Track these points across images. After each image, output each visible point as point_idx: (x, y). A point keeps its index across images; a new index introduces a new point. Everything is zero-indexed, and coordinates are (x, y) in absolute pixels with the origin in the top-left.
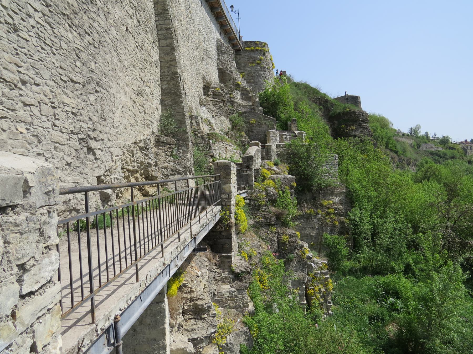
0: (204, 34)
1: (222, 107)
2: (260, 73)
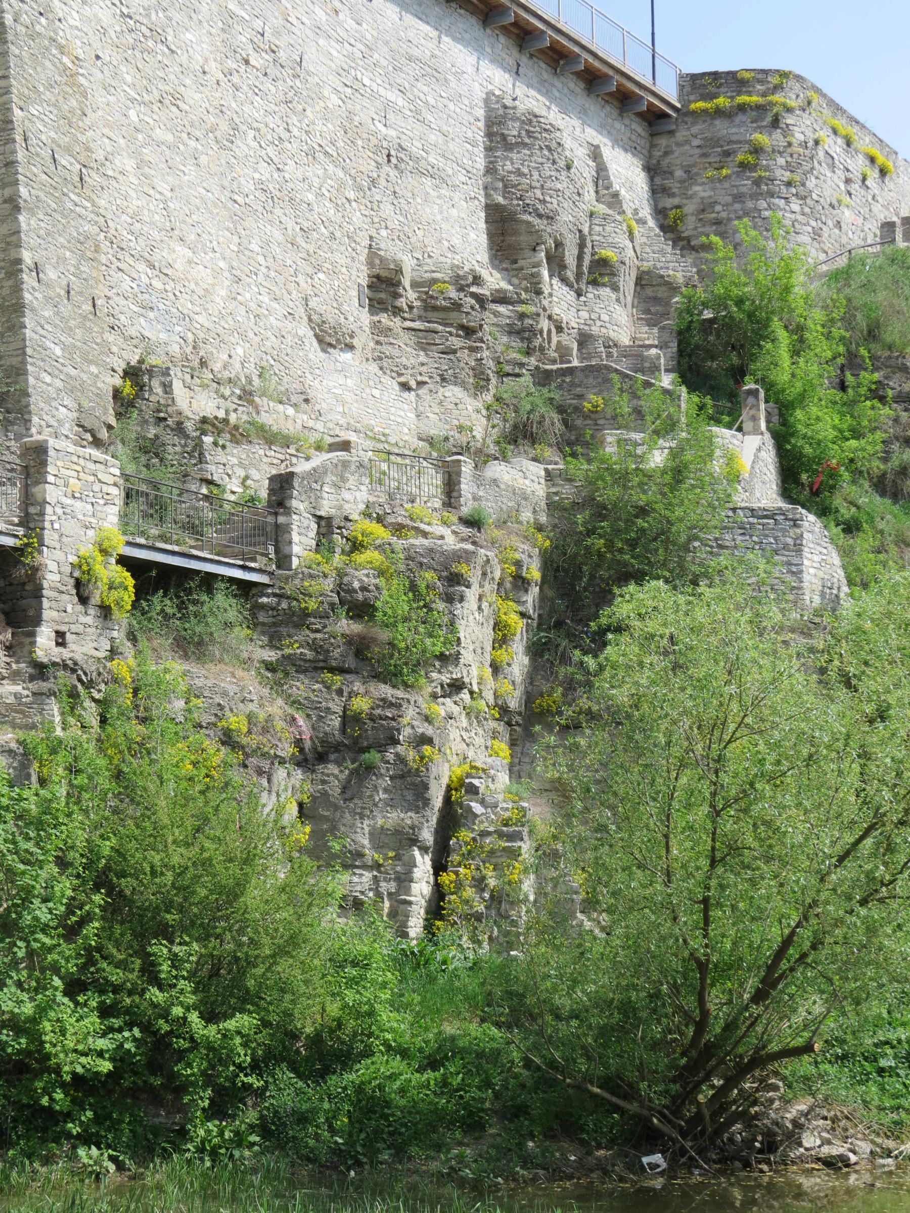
0: (382, 91)
1: (454, 352)
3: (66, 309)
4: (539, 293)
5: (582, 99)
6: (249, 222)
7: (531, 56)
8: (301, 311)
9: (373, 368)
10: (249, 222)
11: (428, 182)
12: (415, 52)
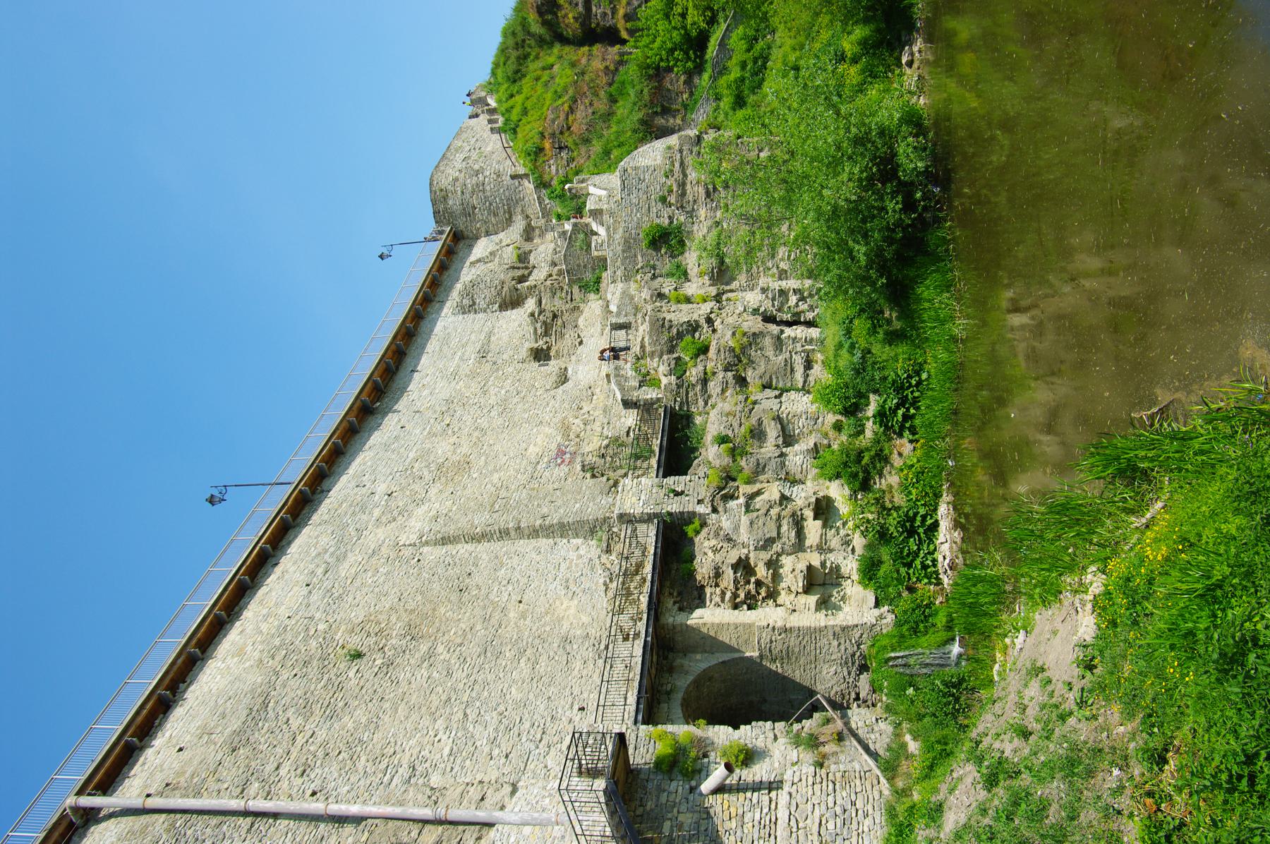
0: (456, 362)
1: (564, 322)
2: (489, 194)
3: (560, 502)
4: (535, 286)
5: (451, 271)
6: (516, 419)
7: (434, 296)
8: (552, 393)
9: (573, 358)
10: (516, 419)
11: (492, 338)
12: (437, 349)
